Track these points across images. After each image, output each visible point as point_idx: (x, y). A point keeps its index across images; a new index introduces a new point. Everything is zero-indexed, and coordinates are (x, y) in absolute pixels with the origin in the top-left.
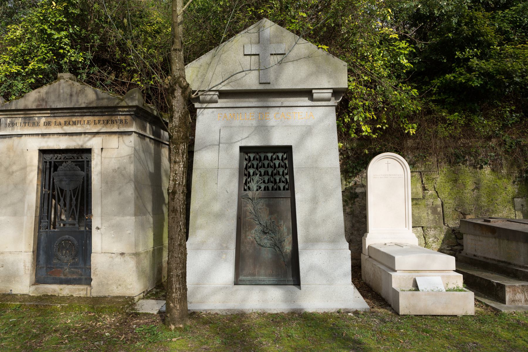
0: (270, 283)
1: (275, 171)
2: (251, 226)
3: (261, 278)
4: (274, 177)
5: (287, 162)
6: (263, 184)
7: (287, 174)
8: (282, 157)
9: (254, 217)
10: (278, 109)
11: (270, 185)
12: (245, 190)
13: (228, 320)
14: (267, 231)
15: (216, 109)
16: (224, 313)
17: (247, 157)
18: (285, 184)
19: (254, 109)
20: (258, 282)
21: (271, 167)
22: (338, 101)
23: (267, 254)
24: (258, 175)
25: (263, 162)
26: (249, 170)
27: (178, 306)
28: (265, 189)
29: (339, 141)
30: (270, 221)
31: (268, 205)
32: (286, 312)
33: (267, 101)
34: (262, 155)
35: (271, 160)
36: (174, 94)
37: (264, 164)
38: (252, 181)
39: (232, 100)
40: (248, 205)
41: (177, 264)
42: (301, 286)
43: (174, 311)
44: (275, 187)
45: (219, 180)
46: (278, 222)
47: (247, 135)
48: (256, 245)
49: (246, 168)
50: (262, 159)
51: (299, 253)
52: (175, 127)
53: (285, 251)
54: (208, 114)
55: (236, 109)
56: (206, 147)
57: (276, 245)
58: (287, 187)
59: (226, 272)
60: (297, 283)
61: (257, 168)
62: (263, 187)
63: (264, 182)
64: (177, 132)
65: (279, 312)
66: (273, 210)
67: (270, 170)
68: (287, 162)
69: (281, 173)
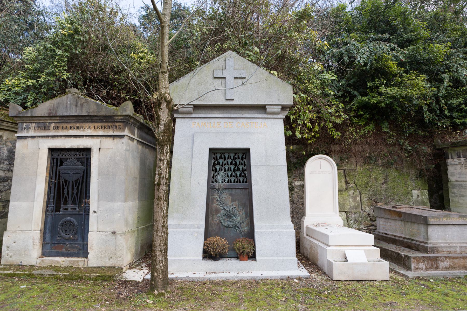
0: (232, 256)
1: (236, 168)
11: (233, 179)
12: (212, 182)
17: (214, 157)
21: (234, 165)
24: (223, 171)
26: (216, 166)
27: (161, 276)
28: (228, 182)
34: (227, 155)
36: (160, 107)
37: (228, 162)
41: (161, 241)
42: (257, 258)
43: (158, 279)
44: (236, 180)
49: (214, 165)
52: (161, 132)
55: (206, 119)
57: (236, 226)
58: (245, 180)
62: (227, 180)
63: (228, 176)
64: (162, 136)
67: (232, 167)
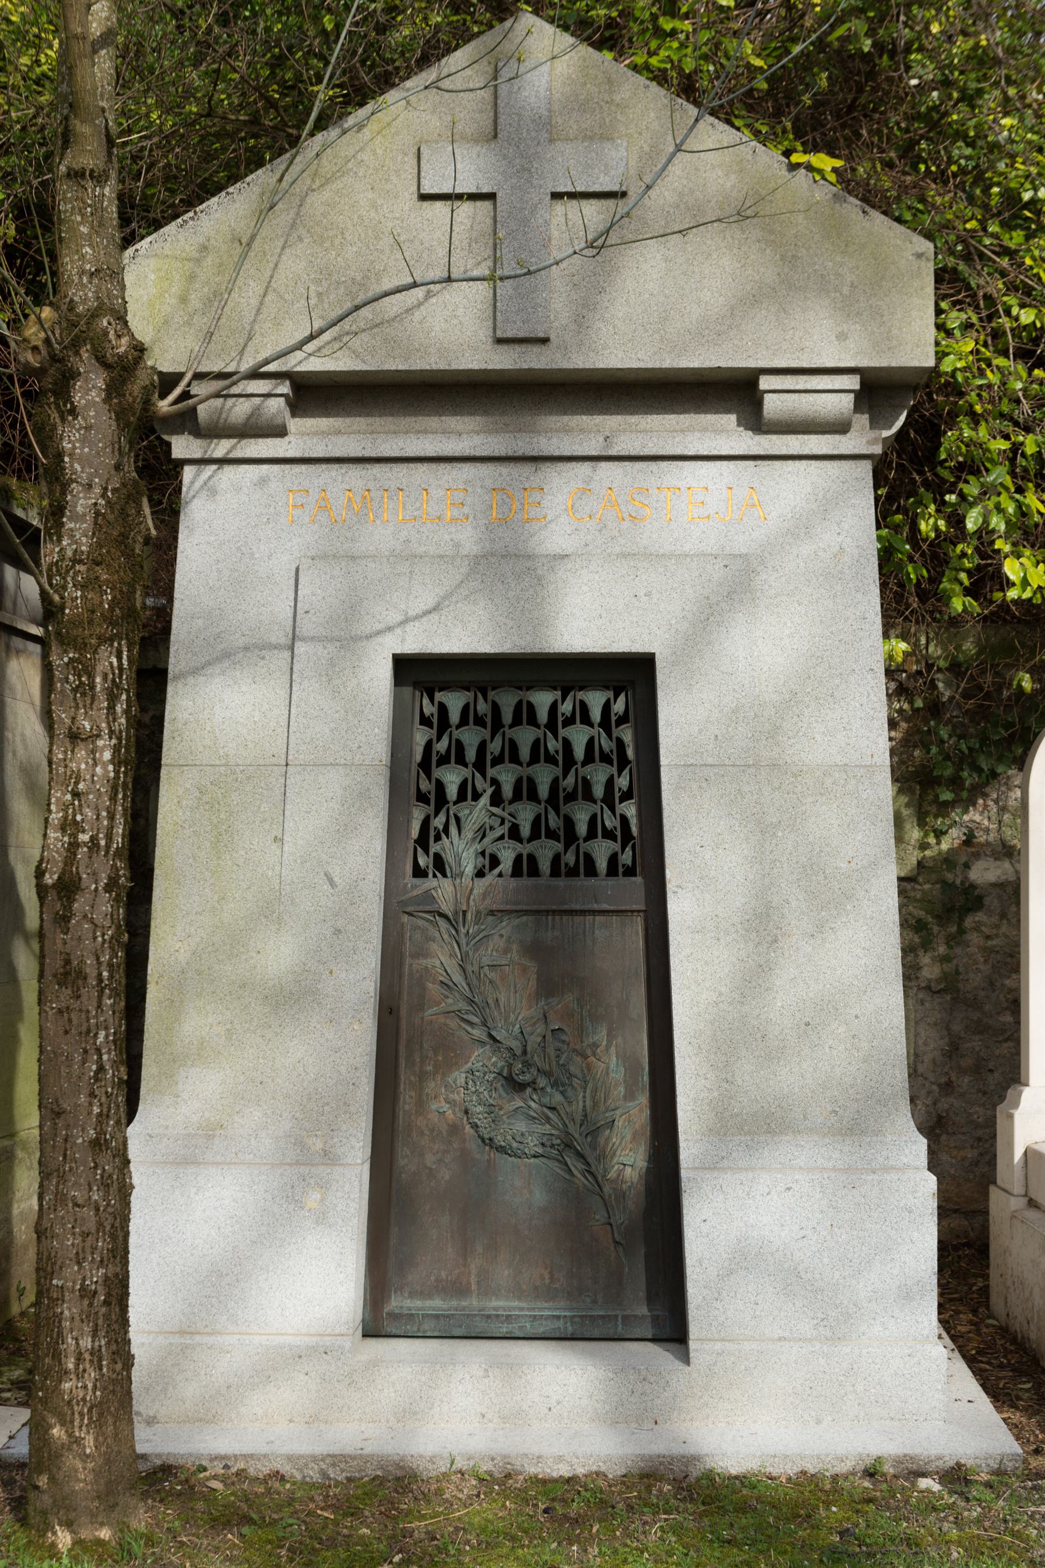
0: (541, 1330)
1: (570, 780)
2: (449, 1053)
3: (496, 1304)
4: (565, 809)
5: (627, 734)
6: (508, 842)
7: (627, 796)
8: (607, 708)
9: (463, 1005)
10: (585, 468)
11: (545, 851)
12: (419, 872)
13: (334, 1508)
14: (527, 1078)
15: (276, 468)
16: (313, 1474)
17: (429, 709)
18: (616, 846)
19: (467, 470)
20: (481, 1326)
21: (551, 760)
22: (886, 433)
23: (525, 1189)
24: (485, 800)
25: (510, 733)
26: (438, 773)
27: (89, 1441)
29: (886, 635)
30: (540, 1029)
31: (535, 950)
32: (614, 1471)
33: (533, 430)
34: (507, 701)
35: (552, 726)
36: (68, 399)
37: (514, 746)
38: (453, 830)
39: (360, 422)
40: (434, 946)
41: (85, 1235)
42: (692, 1345)
43: (71, 1461)
44: (570, 858)
45: (289, 824)
46: (581, 1032)
47: (430, 602)
48: (473, 1145)
49: (425, 765)
50: (507, 717)
51: (685, 1185)
52: (75, 561)
53: (612, 1174)
54: (238, 489)
55: (377, 469)
56: (224, 655)
57: (568, 1146)
58: (626, 858)
59: (324, 1273)
60: (673, 1330)
61: (480, 766)
62: (507, 856)
63: (514, 833)
64: (83, 587)
65: (580, 1471)
66: (558, 973)
67: (544, 776)
68: (627, 734)
69: (599, 791)
